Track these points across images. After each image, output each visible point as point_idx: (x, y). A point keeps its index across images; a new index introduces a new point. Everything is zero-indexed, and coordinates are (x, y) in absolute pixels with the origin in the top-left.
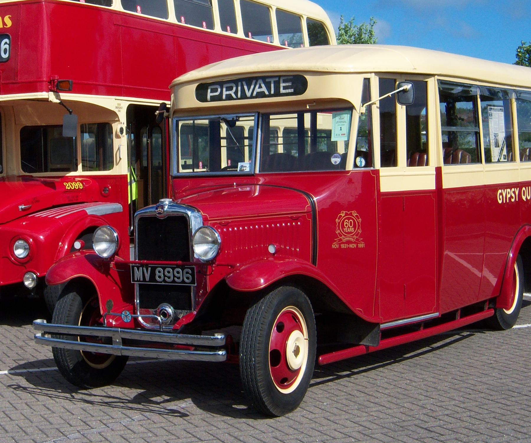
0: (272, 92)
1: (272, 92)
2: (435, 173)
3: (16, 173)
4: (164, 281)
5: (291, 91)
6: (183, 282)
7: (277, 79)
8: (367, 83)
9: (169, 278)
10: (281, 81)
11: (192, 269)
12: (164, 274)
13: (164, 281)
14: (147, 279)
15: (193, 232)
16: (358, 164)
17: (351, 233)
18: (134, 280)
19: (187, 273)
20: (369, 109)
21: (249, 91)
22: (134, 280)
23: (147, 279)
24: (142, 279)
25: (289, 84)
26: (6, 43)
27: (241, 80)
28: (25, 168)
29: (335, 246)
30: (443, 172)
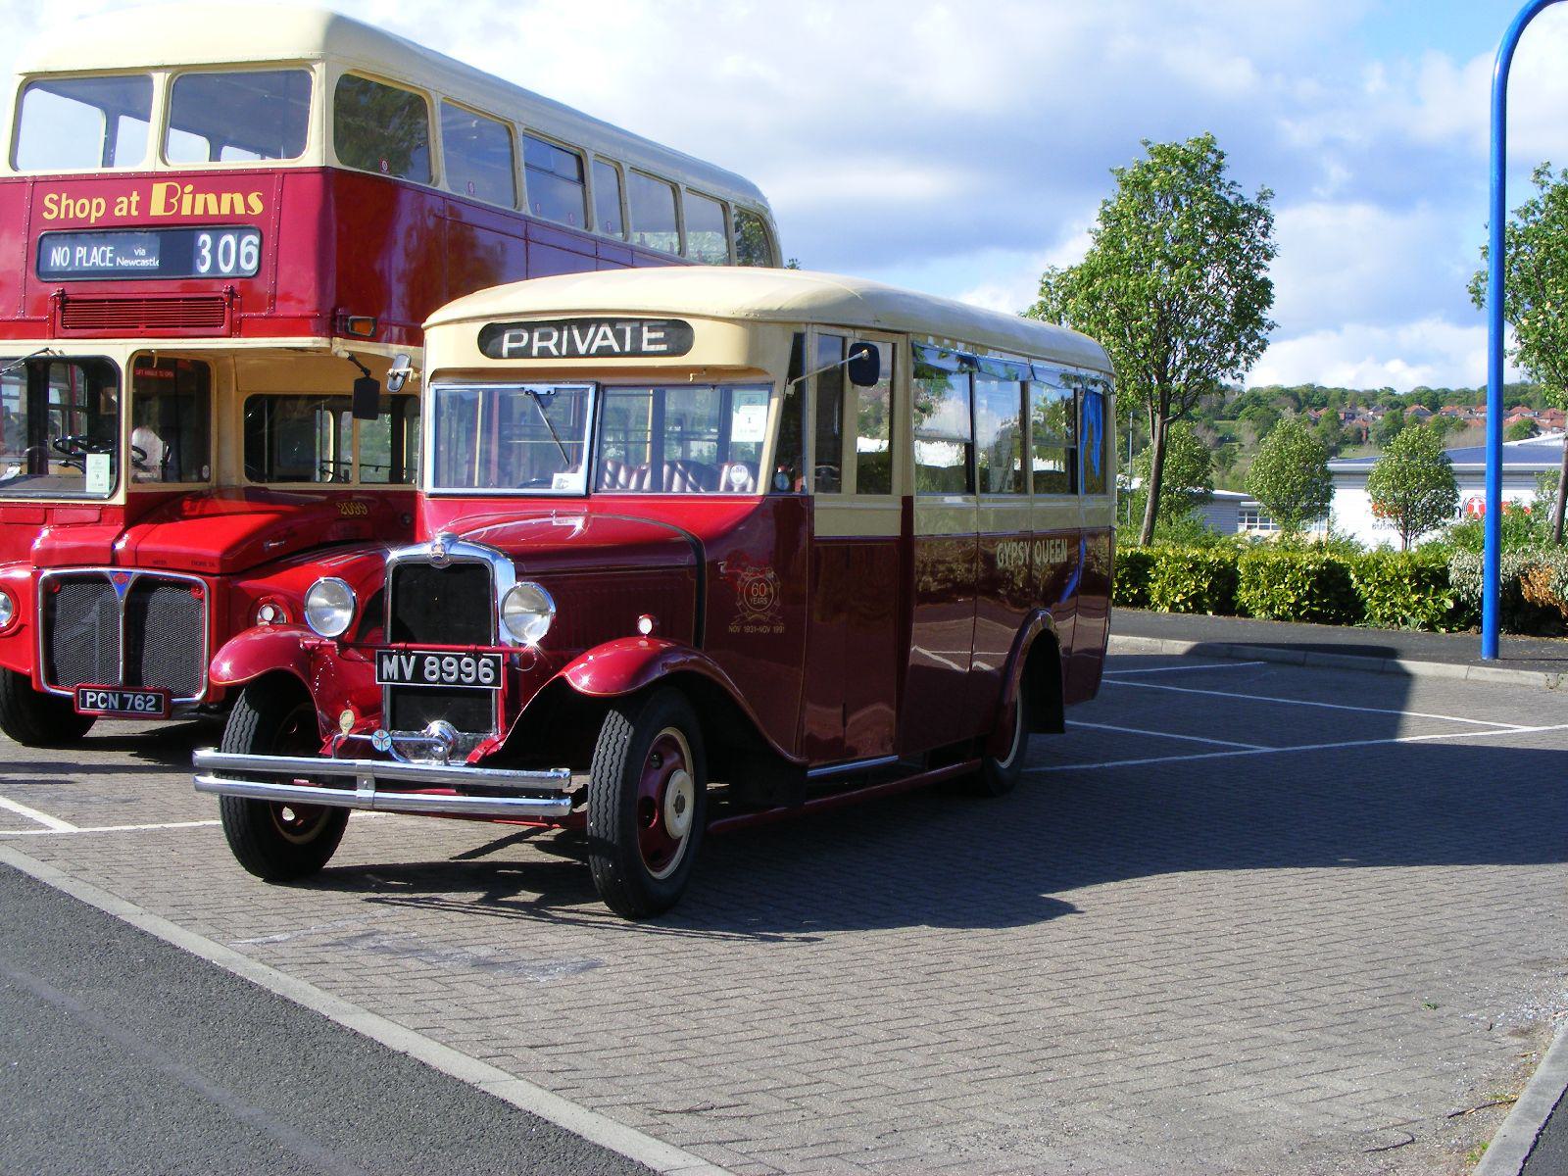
0: (628, 348)
1: (628, 348)
2: (900, 507)
3: (235, 481)
4: (441, 680)
5: (663, 347)
6: (477, 681)
7: (637, 325)
8: (798, 342)
9: (450, 674)
10: (645, 329)
11: (496, 660)
12: (441, 668)
13: (441, 680)
14: (408, 676)
15: (501, 597)
16: (779, 485)
17: (762, 606)
18: (381, 678)
19: (486, 665)
20: (800, 388)
21: (583, 343)
22: (381, 678)
23: (408, 676)
24: (396, 677)
25: (660, 335)
26: (250, 243)
27: (569, 323)
28: (250, 475)
29: (734, 629)
30: (916, 505)
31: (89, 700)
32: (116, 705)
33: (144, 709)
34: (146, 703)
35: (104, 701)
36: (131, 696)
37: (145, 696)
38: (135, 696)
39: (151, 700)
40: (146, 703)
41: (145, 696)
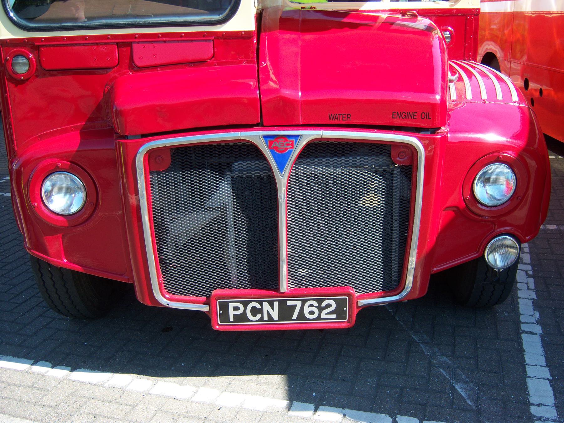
31: (232, 313)
32: (275, 315)
33: (319, 318)
34: (321, 309)
35: (255, 311)
36: (299, 304)
37: (320, 302)
38: (304, 302)
39: (329, 306)
40: (321, 309)
41: (320, 302)
